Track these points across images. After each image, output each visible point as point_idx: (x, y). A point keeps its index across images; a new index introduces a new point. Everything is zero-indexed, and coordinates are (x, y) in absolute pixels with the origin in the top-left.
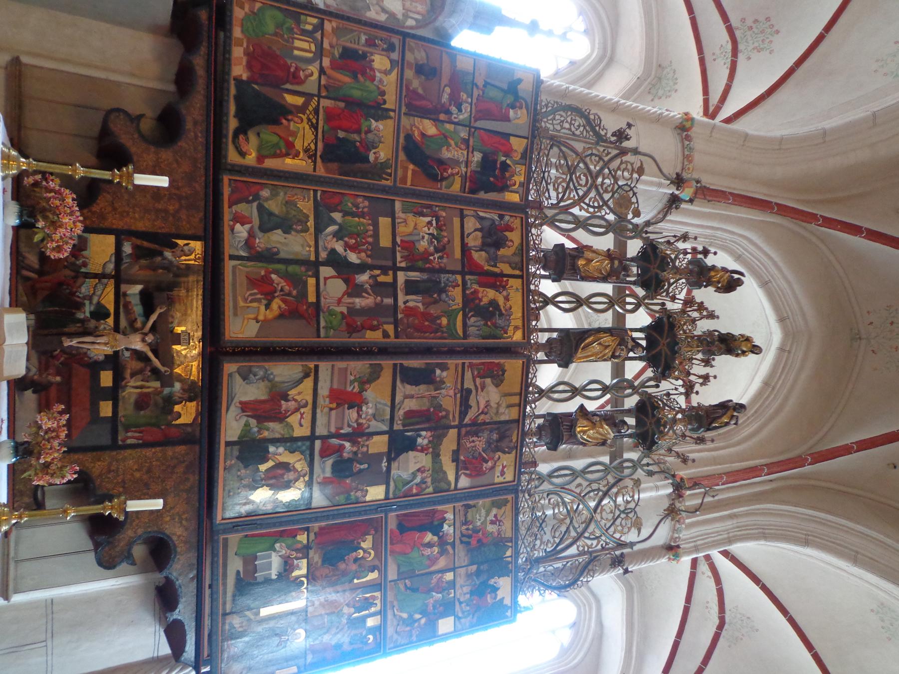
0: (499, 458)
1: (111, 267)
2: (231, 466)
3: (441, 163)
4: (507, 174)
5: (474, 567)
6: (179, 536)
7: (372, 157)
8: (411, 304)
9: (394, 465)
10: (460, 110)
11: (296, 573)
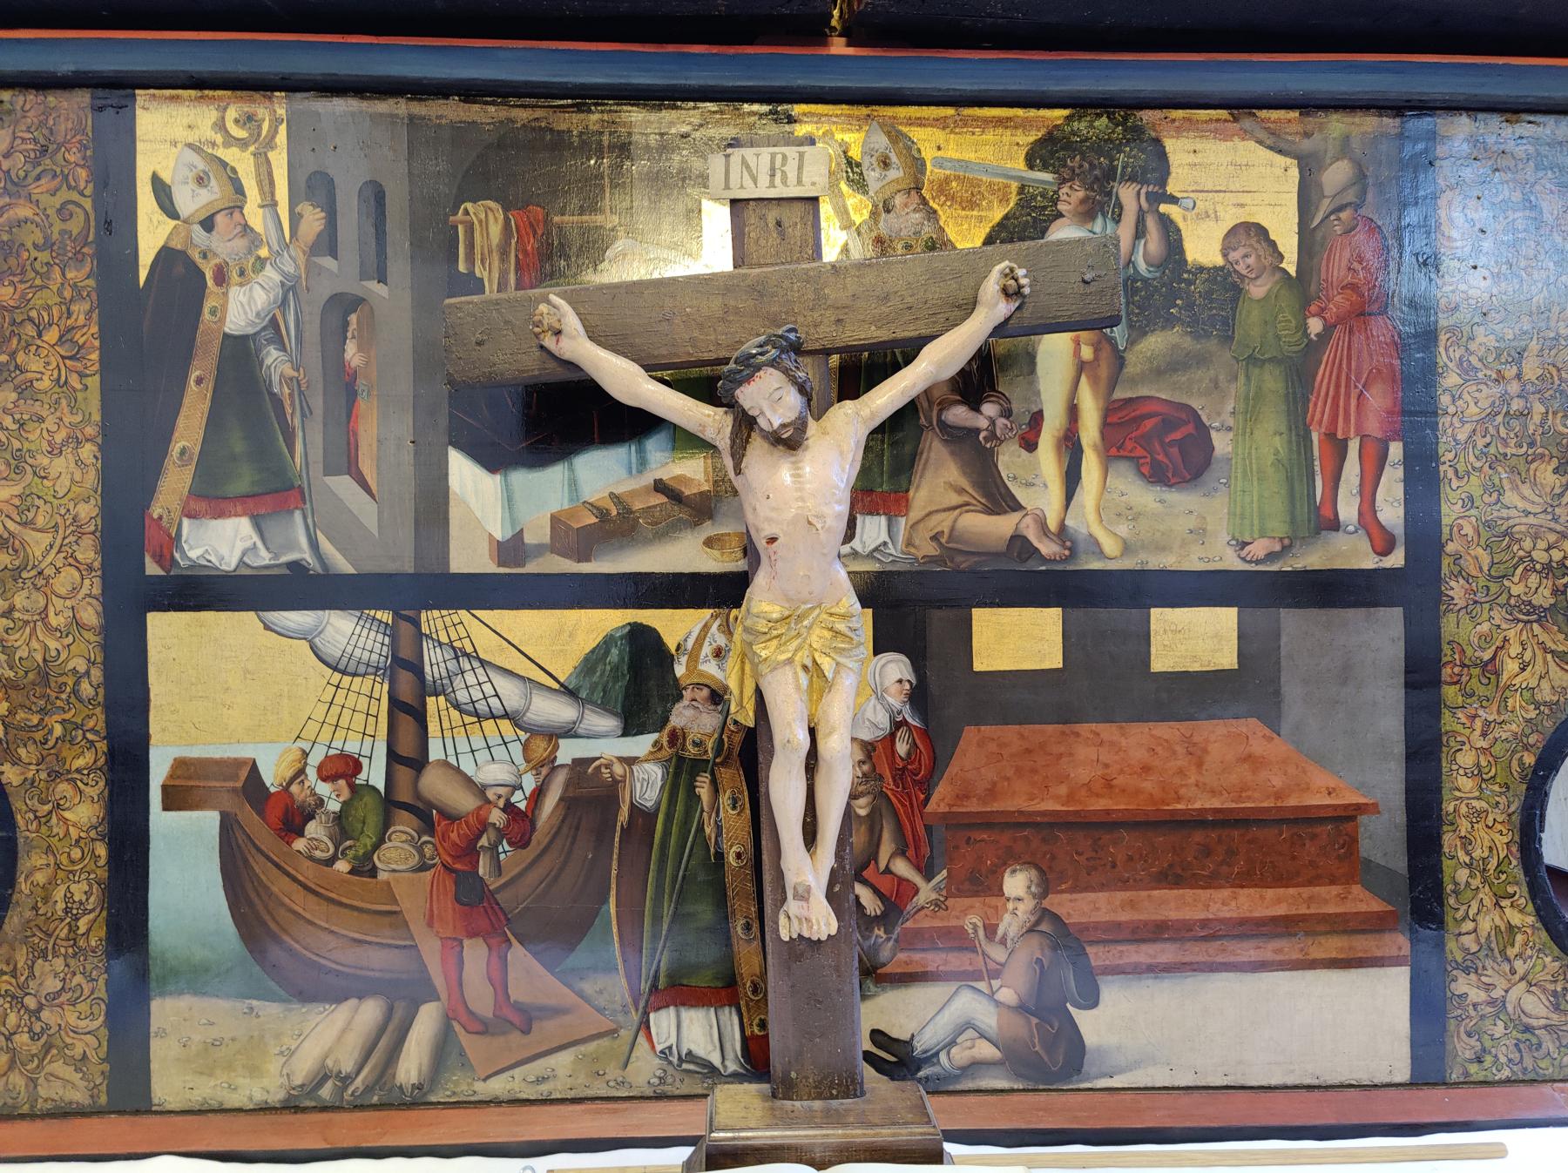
1: (342, 629)
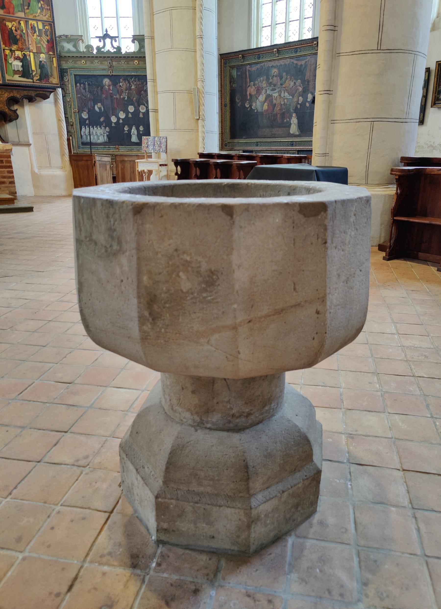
11: (20, 56)
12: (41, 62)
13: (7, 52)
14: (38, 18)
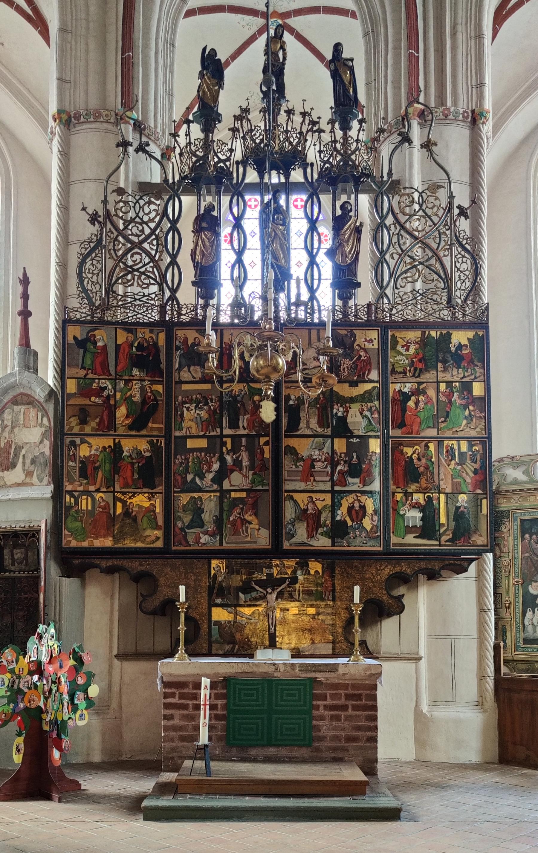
0: (358, 345)
2: (347, 542)
3: (144, 400)
4: (146, 345)
5: (440, 365)
6: (390, 570)
7: (148, 454)
8: (245, 424)
9: (356, 433)
10: (105, 388)
11: (422, 501)
12: (458, 508)
13: (399, 496)
14: (460, 434)
